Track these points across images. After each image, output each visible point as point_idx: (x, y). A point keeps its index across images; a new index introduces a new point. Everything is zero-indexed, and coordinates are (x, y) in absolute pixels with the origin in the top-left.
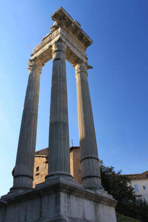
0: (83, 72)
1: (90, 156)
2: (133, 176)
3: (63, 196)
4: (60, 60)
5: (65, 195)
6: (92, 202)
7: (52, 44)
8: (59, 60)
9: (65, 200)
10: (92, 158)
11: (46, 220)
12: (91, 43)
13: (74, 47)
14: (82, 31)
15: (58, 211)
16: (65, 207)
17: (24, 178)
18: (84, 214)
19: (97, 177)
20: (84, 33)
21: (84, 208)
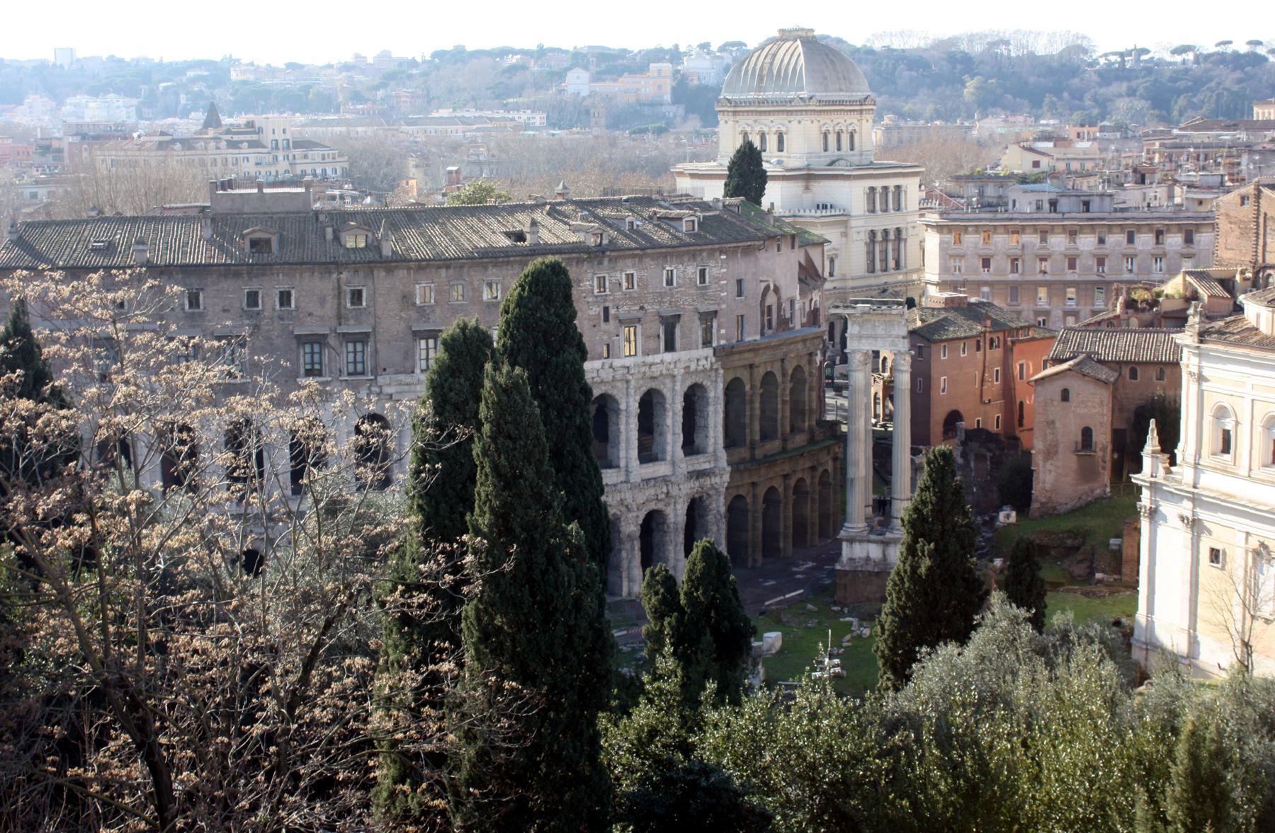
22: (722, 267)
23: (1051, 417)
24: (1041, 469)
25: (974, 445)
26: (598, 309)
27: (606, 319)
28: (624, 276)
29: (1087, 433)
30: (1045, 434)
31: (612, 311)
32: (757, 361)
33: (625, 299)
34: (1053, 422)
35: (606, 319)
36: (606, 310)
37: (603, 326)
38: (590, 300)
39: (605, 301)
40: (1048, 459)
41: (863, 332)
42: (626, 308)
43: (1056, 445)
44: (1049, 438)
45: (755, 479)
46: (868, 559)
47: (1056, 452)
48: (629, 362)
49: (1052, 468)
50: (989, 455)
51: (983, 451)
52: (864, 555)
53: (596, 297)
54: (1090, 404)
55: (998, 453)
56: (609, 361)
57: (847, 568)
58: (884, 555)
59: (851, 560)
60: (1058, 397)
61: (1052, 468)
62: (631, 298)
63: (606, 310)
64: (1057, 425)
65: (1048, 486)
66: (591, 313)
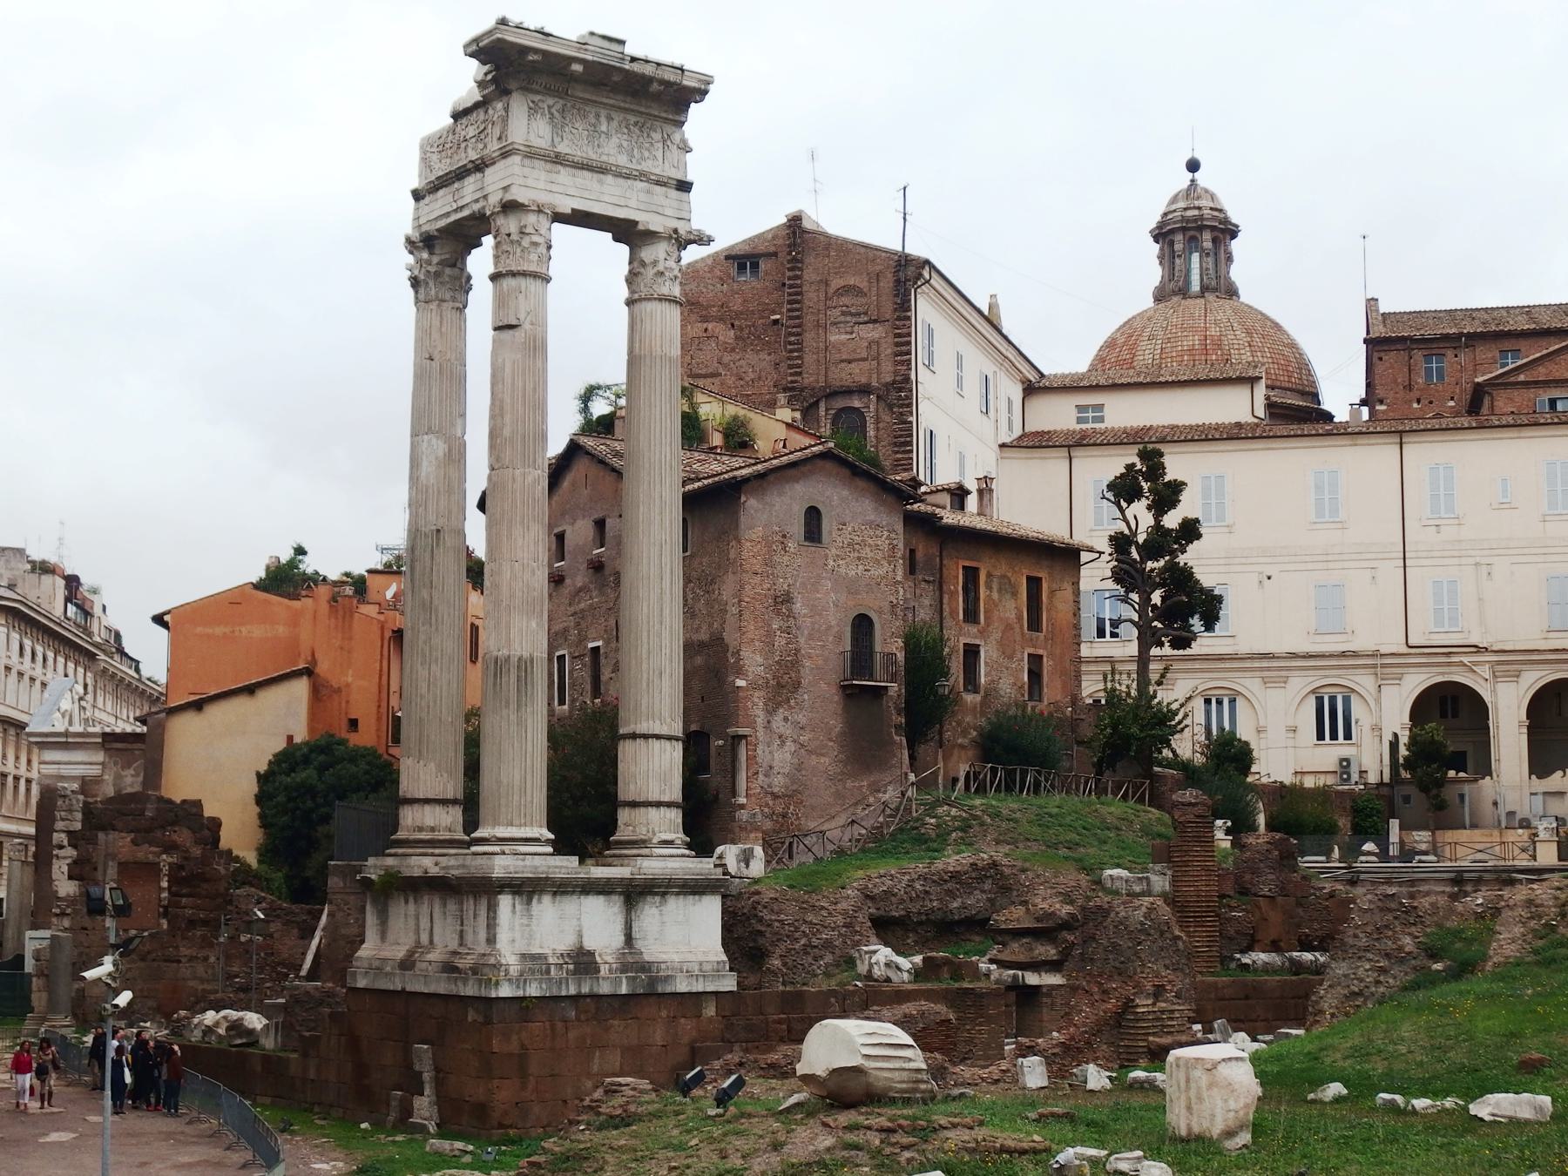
0: (649, 299)
1: (643, 728)
2: (1523, 344)
3: (505, 902)
4: (517, 333)
5: (514, 899)
6: (615, 898)
7: (488, 213)
8: (511, 332)
9: (514, 912)
10: (646, 737)
11: (469, 957)
12: (706, 92)
13: (601, 170)
14: (636, 67)
15: (491, 940)
16: (512, 929)
17: (427, 808)
18: (580, 936)
19: (658, 804)
20: (648, 70)
21: (579, 919)
23: (781, 584)
24: (761, 733)
25: (119, 843)
29: (862, 625)
30: (770, 634)
34: (787, 599)
40: (779, 705)
41: (563, 148)
43: (795, 664)
44: (780, 641)
46: (583, 961)
47: (797, 685)
49: (786, 730)
50: (166, 860)
51: (146, 853)
52: (565, 943)
54: (867, 552)
55: (197, 852)
57: (533, 990)
58: (629, 939)
59: (534, 962)
60: (797, 528)
61: (786, 730)
64: (798, 606)
65: (778, 783)
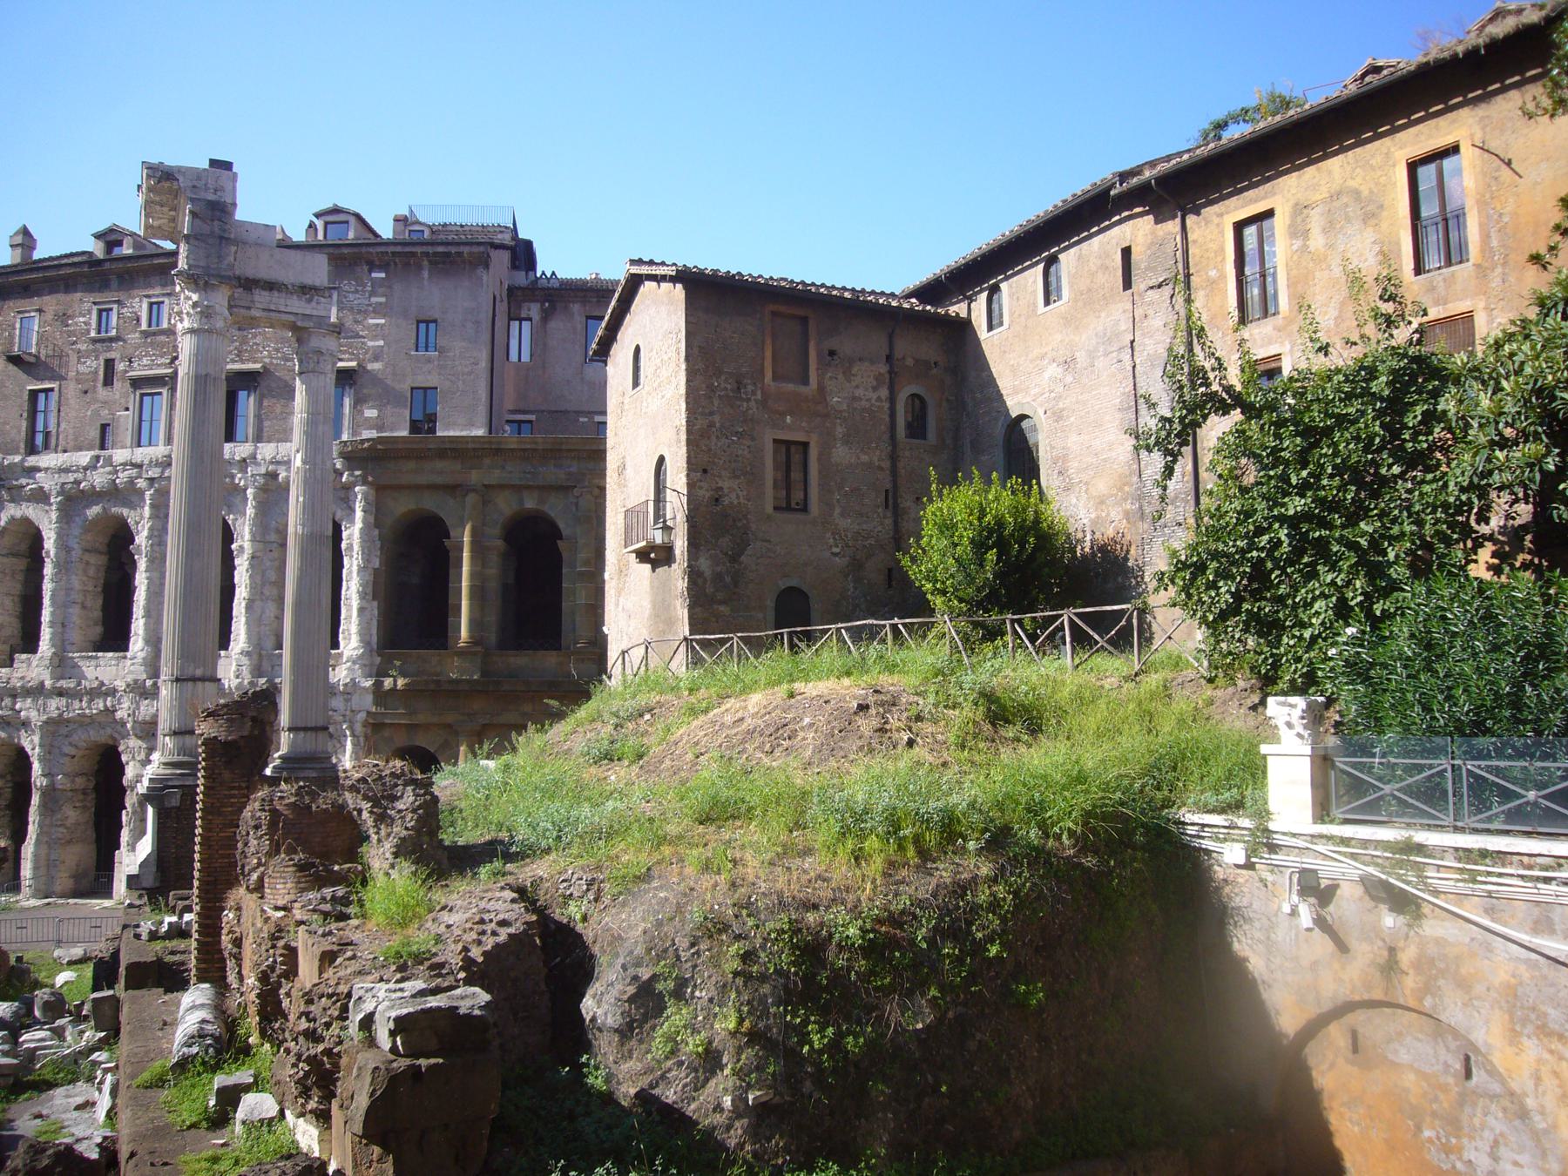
22: (373, 293)
26: (94, 364)
27: (108, 381)
28: (145, 306)
31: (120, 366)
32: (475, 477)
33: (145, 345)
35: (108, 381)
36: (109, 364)
37: (102, 392)
38: (83, 347)
39: (110, 350)
42: (145, 361)
45: (450, 718)
48: (142, 454)
53: (95, 341)
56: (108, 452)
62: (152, 344)
63: (109, 364)
66: (81, 368)
